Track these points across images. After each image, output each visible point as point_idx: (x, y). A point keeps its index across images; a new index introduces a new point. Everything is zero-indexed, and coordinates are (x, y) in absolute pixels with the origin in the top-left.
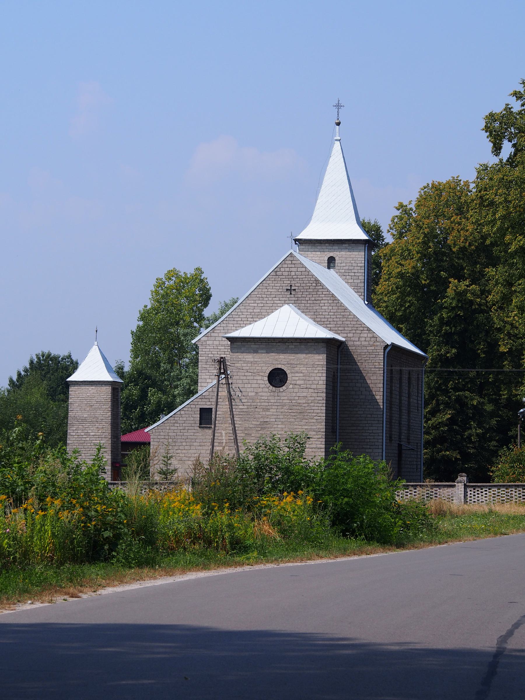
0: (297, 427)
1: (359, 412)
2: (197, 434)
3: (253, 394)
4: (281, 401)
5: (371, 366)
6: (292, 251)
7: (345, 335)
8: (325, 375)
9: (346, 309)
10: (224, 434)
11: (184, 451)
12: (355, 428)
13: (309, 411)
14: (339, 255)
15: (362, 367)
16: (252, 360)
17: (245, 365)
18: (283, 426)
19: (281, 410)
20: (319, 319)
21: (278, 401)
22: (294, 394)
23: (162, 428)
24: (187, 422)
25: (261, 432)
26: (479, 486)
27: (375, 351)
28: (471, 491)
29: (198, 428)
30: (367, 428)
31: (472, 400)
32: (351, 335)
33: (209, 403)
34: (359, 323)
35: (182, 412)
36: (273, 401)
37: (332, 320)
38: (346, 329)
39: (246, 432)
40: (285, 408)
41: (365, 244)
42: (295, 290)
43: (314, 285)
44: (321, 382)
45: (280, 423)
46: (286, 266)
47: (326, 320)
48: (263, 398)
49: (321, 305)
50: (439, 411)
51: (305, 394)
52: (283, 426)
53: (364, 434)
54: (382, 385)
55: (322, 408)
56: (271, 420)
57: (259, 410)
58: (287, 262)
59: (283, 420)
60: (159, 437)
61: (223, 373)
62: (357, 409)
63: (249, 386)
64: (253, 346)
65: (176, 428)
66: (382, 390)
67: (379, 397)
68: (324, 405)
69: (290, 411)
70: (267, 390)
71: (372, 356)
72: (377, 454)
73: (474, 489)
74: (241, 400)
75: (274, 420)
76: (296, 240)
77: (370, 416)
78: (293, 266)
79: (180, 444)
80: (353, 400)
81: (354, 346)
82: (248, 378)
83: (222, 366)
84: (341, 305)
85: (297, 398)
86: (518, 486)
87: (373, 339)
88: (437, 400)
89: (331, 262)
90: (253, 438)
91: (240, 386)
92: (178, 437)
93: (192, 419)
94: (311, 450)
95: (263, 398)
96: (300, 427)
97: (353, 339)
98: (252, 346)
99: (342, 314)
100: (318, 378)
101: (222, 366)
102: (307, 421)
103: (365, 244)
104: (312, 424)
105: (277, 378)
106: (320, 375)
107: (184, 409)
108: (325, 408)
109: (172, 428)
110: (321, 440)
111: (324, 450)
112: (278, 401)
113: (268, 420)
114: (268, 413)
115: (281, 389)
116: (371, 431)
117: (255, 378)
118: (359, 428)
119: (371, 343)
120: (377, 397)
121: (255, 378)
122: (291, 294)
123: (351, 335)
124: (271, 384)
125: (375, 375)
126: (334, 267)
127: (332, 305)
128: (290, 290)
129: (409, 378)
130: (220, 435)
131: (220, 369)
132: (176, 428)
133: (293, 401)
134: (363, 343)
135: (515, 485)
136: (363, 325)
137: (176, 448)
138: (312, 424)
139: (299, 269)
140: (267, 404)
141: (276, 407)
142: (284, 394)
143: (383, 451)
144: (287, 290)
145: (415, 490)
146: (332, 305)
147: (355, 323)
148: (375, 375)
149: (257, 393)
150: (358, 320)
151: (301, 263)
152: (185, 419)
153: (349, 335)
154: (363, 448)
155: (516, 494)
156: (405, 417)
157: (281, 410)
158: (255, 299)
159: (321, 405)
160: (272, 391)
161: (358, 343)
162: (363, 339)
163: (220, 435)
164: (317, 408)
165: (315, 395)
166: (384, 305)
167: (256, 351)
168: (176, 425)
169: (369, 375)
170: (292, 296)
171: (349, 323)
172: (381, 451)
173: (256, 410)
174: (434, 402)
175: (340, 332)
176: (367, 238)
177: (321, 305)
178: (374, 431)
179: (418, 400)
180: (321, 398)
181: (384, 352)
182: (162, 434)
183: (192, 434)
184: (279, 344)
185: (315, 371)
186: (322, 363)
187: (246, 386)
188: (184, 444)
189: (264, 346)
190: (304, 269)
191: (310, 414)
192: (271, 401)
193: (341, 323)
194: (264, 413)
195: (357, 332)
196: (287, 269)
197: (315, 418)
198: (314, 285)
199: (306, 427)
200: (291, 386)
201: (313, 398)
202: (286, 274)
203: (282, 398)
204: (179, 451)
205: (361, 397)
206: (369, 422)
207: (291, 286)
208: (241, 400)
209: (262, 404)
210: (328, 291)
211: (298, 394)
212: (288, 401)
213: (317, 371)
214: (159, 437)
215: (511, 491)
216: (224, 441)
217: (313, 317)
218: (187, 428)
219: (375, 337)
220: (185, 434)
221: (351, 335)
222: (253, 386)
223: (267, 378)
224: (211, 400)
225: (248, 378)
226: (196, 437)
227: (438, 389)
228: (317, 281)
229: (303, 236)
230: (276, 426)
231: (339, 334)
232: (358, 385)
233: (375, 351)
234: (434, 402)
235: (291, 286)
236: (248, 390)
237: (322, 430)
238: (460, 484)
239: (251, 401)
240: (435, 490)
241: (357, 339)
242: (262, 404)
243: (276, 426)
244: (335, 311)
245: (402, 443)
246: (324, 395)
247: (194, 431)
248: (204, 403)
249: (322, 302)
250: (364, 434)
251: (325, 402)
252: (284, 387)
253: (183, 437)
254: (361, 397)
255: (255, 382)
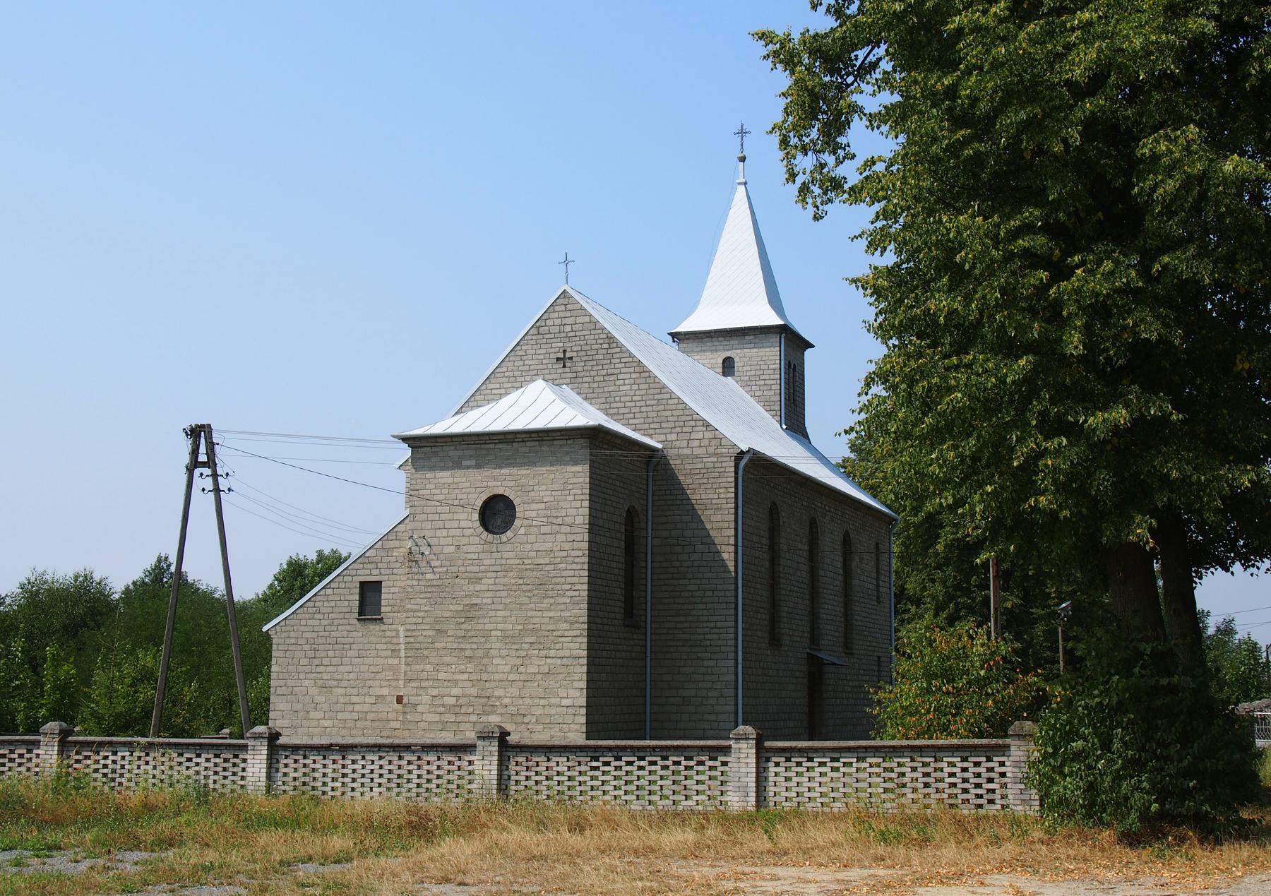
0: (534, 613)
1: (689, 588)
2: (355, 634)
3: (452, 549)
4: (503, 562)
5: (711, 496)
6: (566, 287)
7: (663, 438)
8: (586, 504)
9: (665, 387)
10: (402, 634)
11: (330, 669)
12: (682, 619)
13: (557, 580)
14: (742, 354)
15: (694, 498)
16: (451, 480)
17: (438, 491)
18: (508, 613)
19: (503, 581)
20: (615, 411)
21: (498, 562)
22: (529, 547)
23: (292, 623)
24: (336, 610)
25: (463, 627)
26: (801, 751)
27: (718, 465)
28: (777, 764)
29: (356, 622)
30: (705, 619)
31: (1006, 600)
32: (674, 436)
33: (376, 572)
34: (687, 412)
35: (329, 591)
36: (487, 562)
37: (637, 410)
38: (664, 425)
39: (438, 627)
40: (511, 574)
41: (781, 334)
42: (571, 358)
43: (606, 346)
44: (579, 520)
45: (501, 607)
46: (556, 315)
47: (627, 410)
48: (469, 556)
49: (618, 383)
50: (959, 618)
51: (548, 546)
52: (508, 613)
53: (699, 631)
54: (732, 532)
55: (582, 573)
56: (485, 601)
57: (462, 582)
58: (557, 308)
59: (507, 601)
60: (288, 641)
61: (204, 465)
62: (686, 582)
63: (445, 533)
64: (454, 453)
65: (317, 622)
66: (732, 541)
67: (728, 555)
68: (586, 566)
69: (521, 581)
70: (477, 540)
71: (713, 475)
72: (725, 670)
73: (788, 760)
74: (428, 562)
75: (489, 601)
76: (674, 336)
77: (710, 594)
78: (568, 314)
79: (323, 654)
80: (677, 564)
81: (678, 456)
82: (443, 517)
83: (203, 449)
84: (655, 380)
85: (533, 554)
86: (920, 749)
87: (714, 442)
88: (957, 604)
89: (728, 367)
90: (450, 639)
91: (428, 534)
92: (320, 641)
93: (346, 603)
94: (559, 661)
95: (469, 556)
96: (539, 614)
97: (677, 444)
98: (450, 454)
99: (657, 397)
100: (573, 512)
101: (203, 449)
102: (552, 601)
103: (781, 334)
104: (563, 607)
105: (496, 514)
106: (578, 504)
107: (333, 585)
108: (586, 573)
109: (310, 622)
110: (579, 640)
111: (585, 661)
112: (498, 562)
113: (478, 601)
114: (478, 587)
115: (504, 538)
116: (712, 625)
117: (456, 516)
118: (690, 619)
119: (711, 450)
120: (725, 556)
121: (456, 516)
122: (564, 366)
123: (674, 436)
124: (487, 530)
125: (718, 510)
126: (732, 374)
127: (638, 381)
128: (563, 359)
129: (847, 541)
130: (394, 634)
131: (195, 452)
132: (317, 622)
133: (526, 562)
134: (697, 451)
135: (913, 748)
136: (695, 417)
137: (316, 662)
138: (563, 607)
139: (580, 320)
140: (476, 569)
141: (494, 575)
142: (509, 547)
143: (737, 663)
144: (558, 359)
145: (618, 763)
146: (638, 381)
147: (680, 413)
148: (718, 510)
149: (458, 547)
150: (686, 408)
151: (582, 309)
152: (333, 604)
153: (670, 437)
154: (698, 658)
155: (915, 775)
156: (831, 608)
157: (503, 581)
158: (501, 380)
159: (579, 567)
160: (486, 542)
161: (686, 451)
162: (696, 443)
163: (394, 634)
164: (571, 573)
165: (567, 546)
166: (881, 475)
167: (457, 465)
168: (317, 616)
169: (707, 512)
170: (567, 370)
171: (669, 413)
172: (732, 663)
173: (457, 581)
174: (951, 605)
175: (652, 432)
176: (782, 323)
177: (618, 383)
178: (719, 624)
179: (878, 586)
180: (580, 553)
181: (736, 467)
182: (292, 634)
183: (345, 634)
184: (500, 446)
185: (569, 498)
186: (581, 480)
187: (439, 533)
188: (331, 654)
189: (472, 452)
190: (587, 319)
191: (559, 587)
192: (486, 562)
193: (654, 414)
194: (471, 588)
195: (685, 429)
196: (558, 322)
197: (569, 594)
198: (606, 346)
199: (551, 614)
200: (522, 531)
201: (563, 554)
202: (556, 329)
203: (506, 555)
204: (322, 669)
205: (695, 557)
206: (709, 606)
207: (565, 352)
208: (428, 562)
209: (469, 569)
210: (631, 356)
211: (536, 547)
212: (517, 561)
213: (572, 497)
214: (288, 641)
215: (899, 765)
216: (403, 646)
217: (604, 406)
218: (336, 622)
219: (718, 438)
220: (333, 634)
221: (673, 437)
222: (452, 532)
223: (476, 516)
224: (380, 565)
225: (443, 517)
226: (351, 640)
227: (957, 587)
228: (611, 339)
229: (683, 328)
230: (492, 613)
231: (650, 436)
232: (688, 533)
233: (718, 465)
234: (951, 605)
235: (565, 352)
236: (443, 541)
237: (582, 619)
238: (743, 745)
239: (448, 563)
240: (675, 763)
241: (684, 444)
242: (469, 569)
243: (492, 613)
244: (643, 392)
245: (821, 655)
246: (586, 545)
247: (348, 628)
248: (367, 572)
249: (620, 377)
250: (699, 631)
251: (586, 560)
252: (509, 534)
253: (329, 641)
254: (695, 557)
255: (455, 524)
